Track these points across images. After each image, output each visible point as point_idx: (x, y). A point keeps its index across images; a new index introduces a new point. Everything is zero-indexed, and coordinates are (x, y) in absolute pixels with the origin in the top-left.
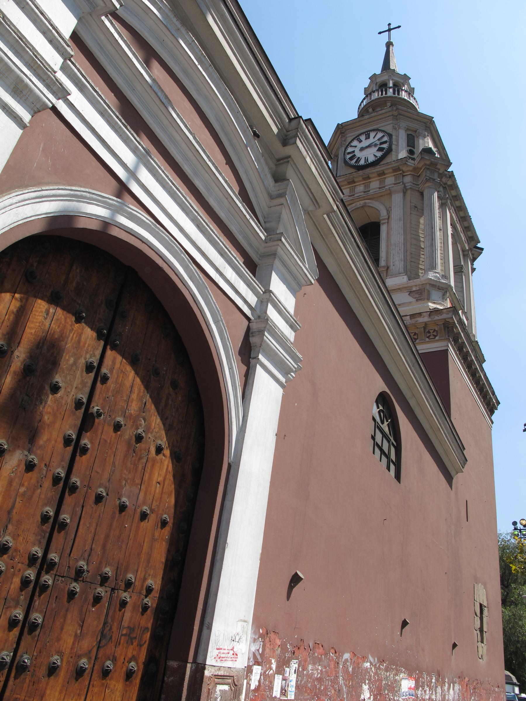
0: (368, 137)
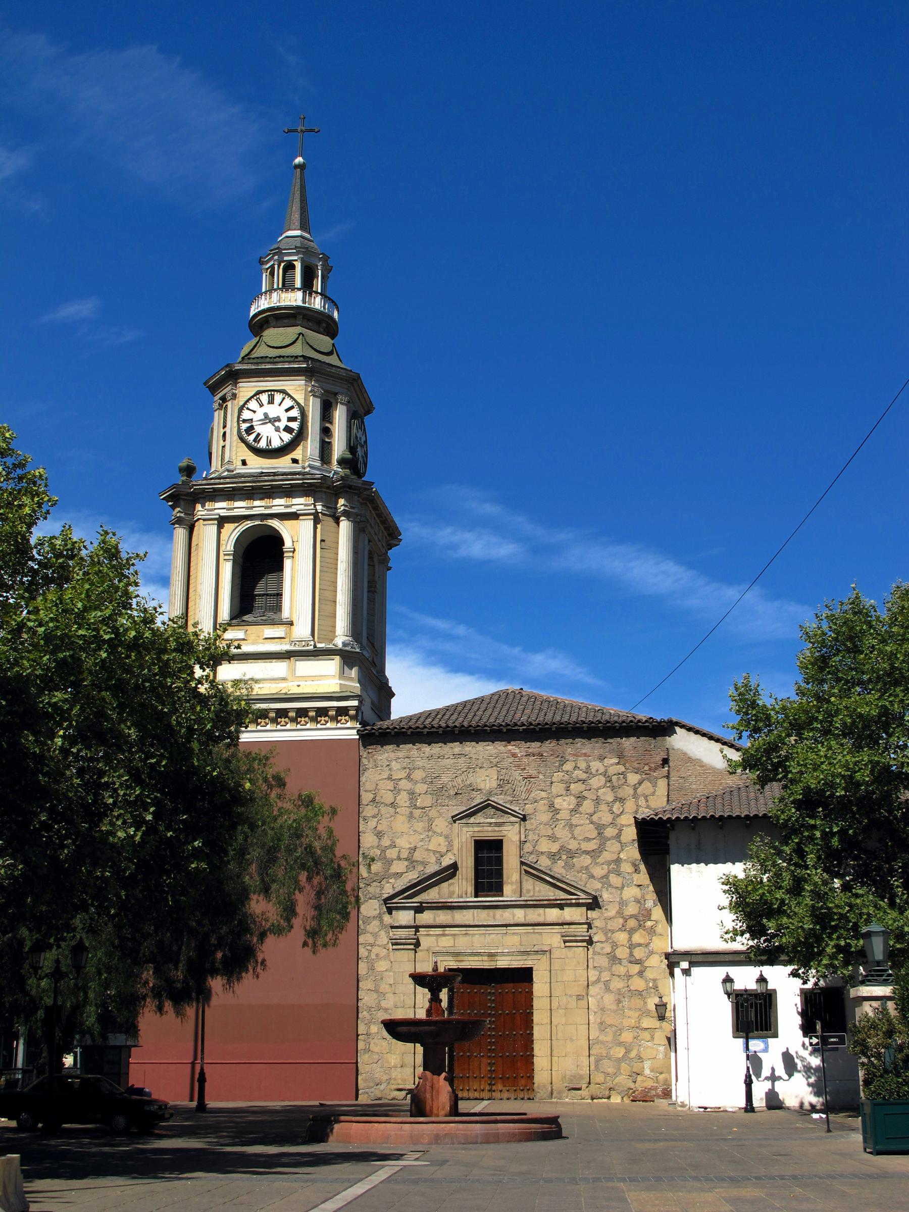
0: (271, 401)
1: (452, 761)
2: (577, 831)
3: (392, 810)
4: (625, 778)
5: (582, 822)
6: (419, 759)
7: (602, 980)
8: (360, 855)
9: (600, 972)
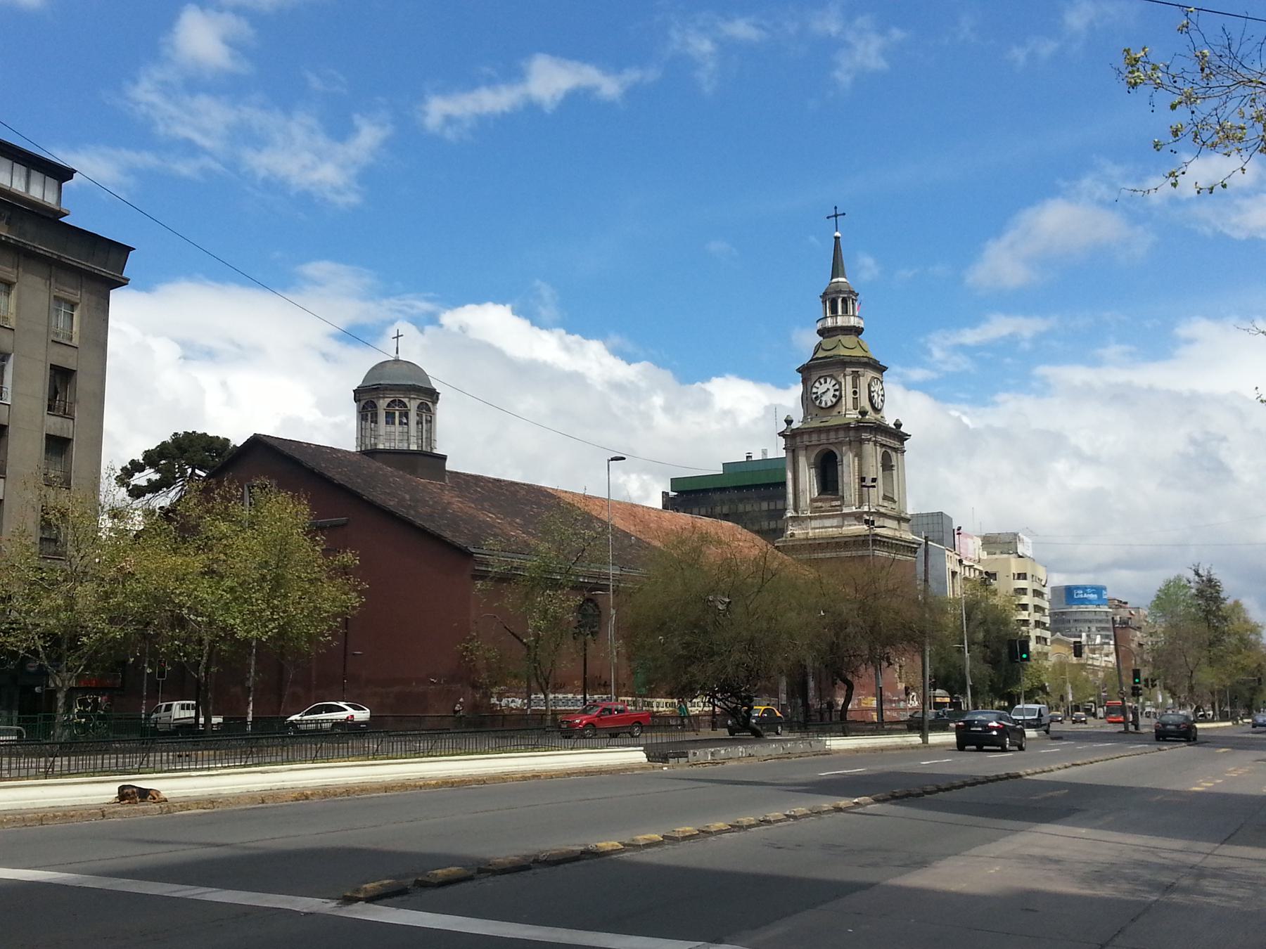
0: (826, 382)
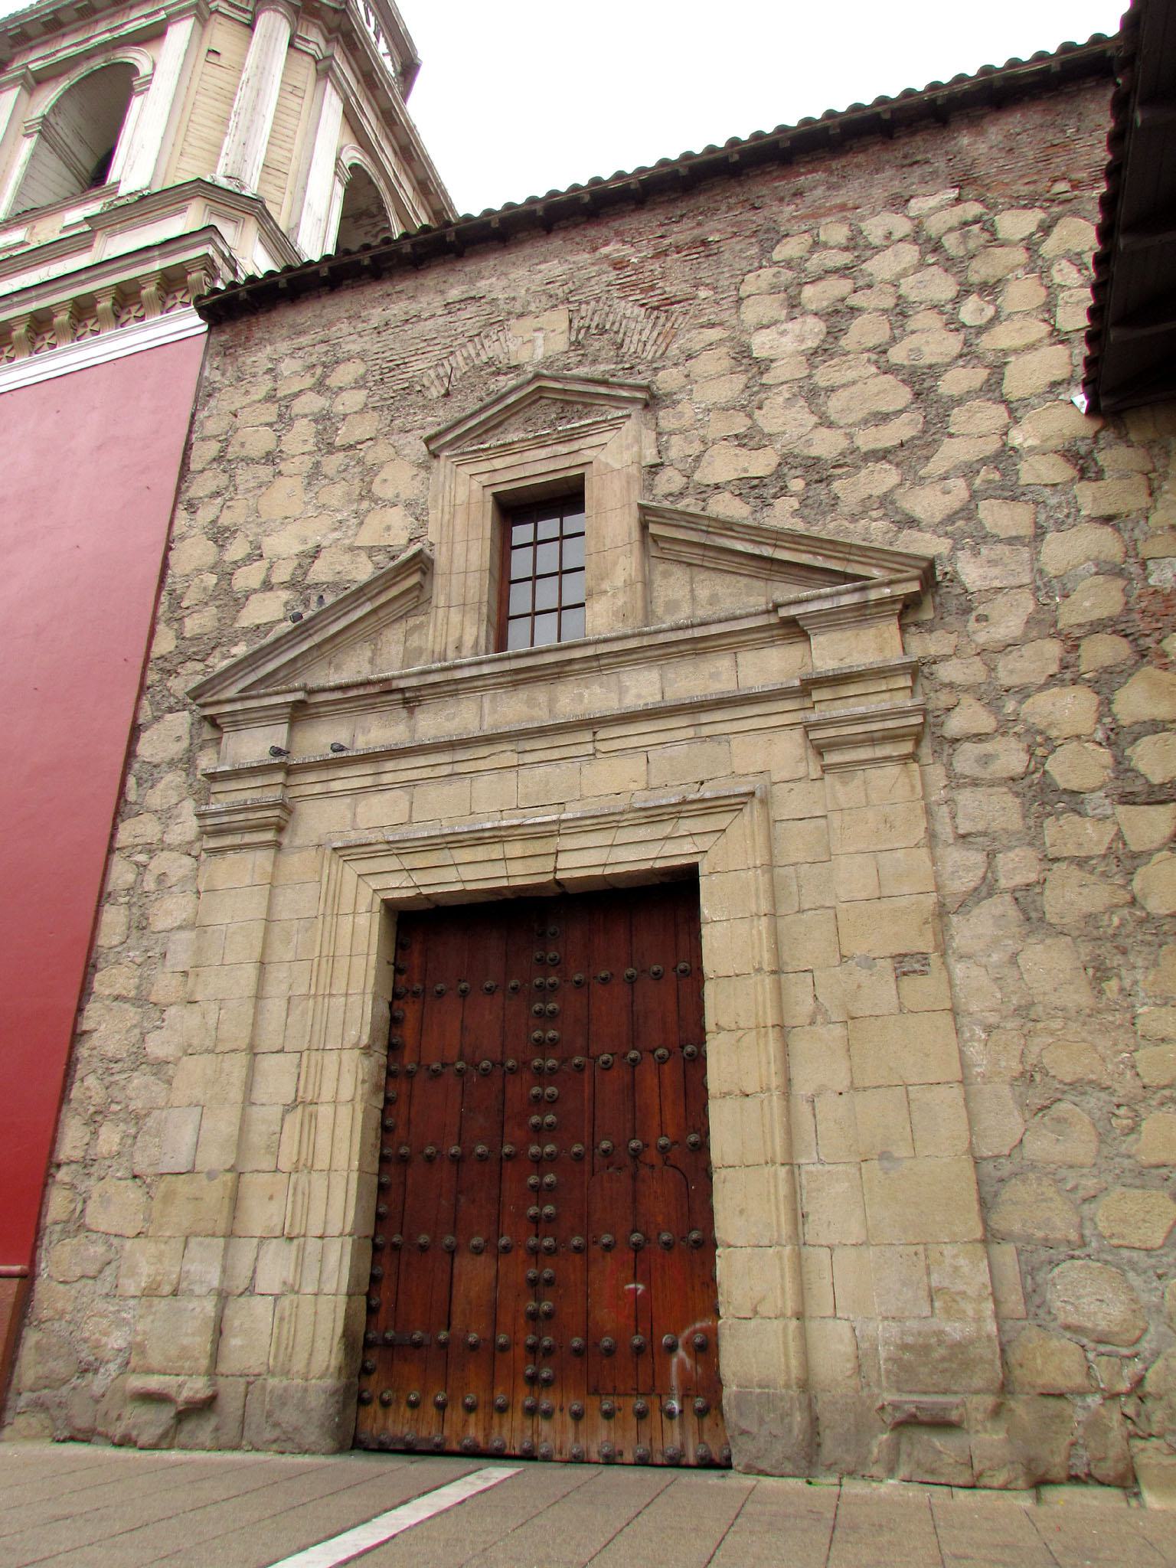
1: (441, 320)
2: (834, 405)
3: (265, 472)
4: (990, 229)
5: (851, 375)
6: (355, 337)
7: (1003, 883)
8: (164, 598)
9: (991, 855)
